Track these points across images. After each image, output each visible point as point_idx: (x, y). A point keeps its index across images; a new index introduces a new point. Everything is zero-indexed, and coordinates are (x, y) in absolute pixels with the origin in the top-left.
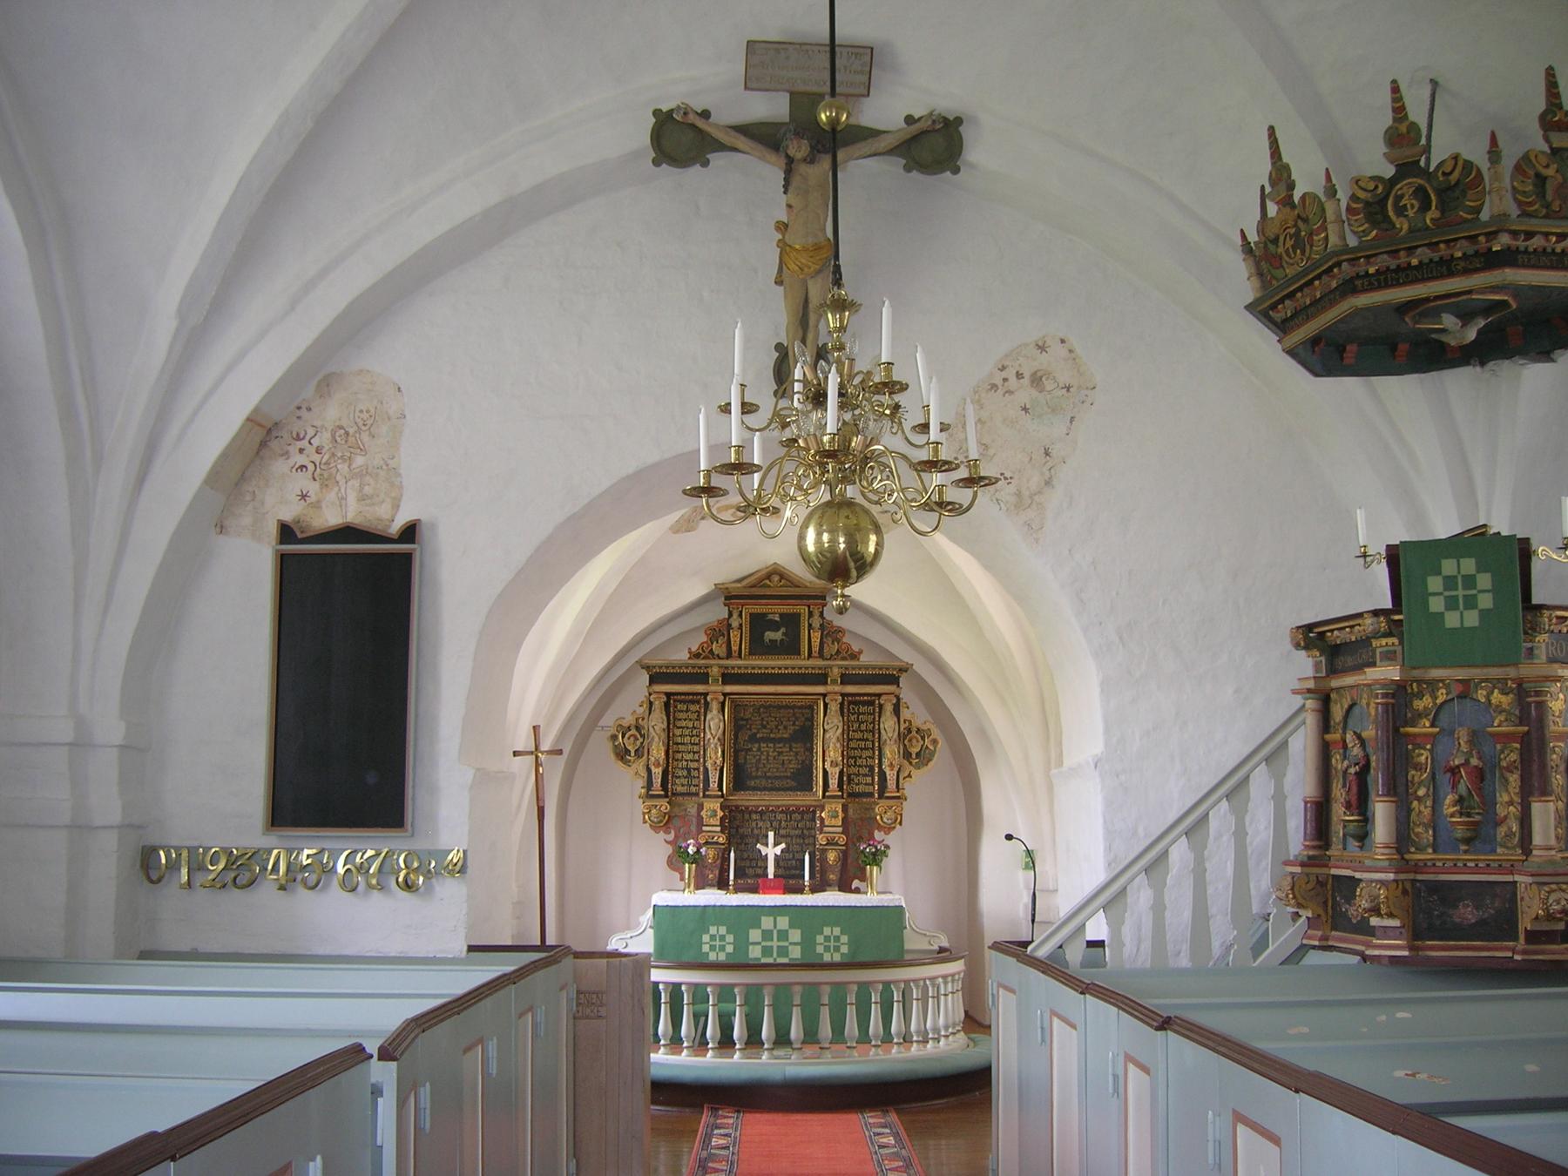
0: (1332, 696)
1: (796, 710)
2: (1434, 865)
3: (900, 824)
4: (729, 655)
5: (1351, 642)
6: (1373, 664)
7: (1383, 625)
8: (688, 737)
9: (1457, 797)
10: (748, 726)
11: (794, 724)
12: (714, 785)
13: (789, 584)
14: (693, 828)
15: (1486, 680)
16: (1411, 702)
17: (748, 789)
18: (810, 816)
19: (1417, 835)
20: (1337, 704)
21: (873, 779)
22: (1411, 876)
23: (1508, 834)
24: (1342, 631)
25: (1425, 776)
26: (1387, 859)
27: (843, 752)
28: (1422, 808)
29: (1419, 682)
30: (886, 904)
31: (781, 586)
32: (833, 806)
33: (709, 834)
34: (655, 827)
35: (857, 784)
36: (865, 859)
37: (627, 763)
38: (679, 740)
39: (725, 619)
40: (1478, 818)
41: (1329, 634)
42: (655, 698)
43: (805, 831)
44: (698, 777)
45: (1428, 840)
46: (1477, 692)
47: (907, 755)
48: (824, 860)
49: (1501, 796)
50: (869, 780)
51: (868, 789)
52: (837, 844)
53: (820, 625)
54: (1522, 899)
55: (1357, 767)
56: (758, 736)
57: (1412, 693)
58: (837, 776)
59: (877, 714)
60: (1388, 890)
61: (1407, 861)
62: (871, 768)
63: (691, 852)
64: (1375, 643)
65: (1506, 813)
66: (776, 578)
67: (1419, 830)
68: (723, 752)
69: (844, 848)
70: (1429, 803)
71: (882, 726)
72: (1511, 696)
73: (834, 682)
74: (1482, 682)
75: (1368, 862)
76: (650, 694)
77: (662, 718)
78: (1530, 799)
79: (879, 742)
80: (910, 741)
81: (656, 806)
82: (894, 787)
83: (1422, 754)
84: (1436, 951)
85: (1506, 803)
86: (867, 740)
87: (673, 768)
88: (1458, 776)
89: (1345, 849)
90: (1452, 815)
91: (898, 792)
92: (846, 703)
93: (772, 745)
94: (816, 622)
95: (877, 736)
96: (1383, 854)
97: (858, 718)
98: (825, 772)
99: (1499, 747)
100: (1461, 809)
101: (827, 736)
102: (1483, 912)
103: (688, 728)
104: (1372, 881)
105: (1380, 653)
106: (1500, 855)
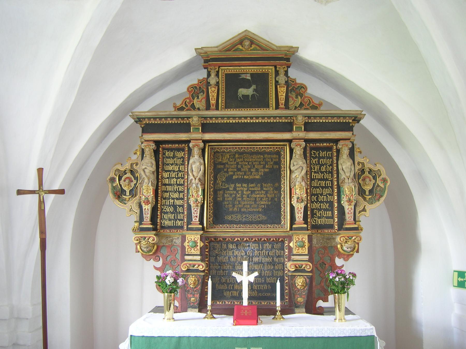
1: (266, 156)
3: (358, 251)
4: (208, 107)
8: (175, 180)
10: (225, 170)
11: (264, 167)
12: (195, 219)
13: (258, 48)
14: (178, 256)
17: (223, 223)
18: (279, 245)
21: (333, 214)
27: (307, 189)
30: (358, 335)
31: (251, 50)
32: (300, 237)
33: (191, 262)
34: (146, 256)
35: (319, 218)
36: (333, 287)
37: (123, 201)
38: (167, 181)
39: (204, 78)
42: (145, 146)
43: (275, 259)
44: (183, 213)
47: (361, 192)
48: (292, 285)
50: (329, 214)
51: (330, 221)
52: (304, 271)
53: (286, 82)
56: (234, 177)
58: (302, 211)
59: (335, 158)
62: (331, 204)
63: (168, 283)
66: (247, 43)
68: (204, 191)
69: (310, 274)
71: (340, 167)
73: (299, 129)
76: (142, 143)
77: (152, 163)
79: (338, 181)
80: (364, 180)
81: (145, 238)
82: (352, 220)
86: (327, 180)
87: (161, 205)
91: (355, 223)
92: (308, 149)
93: (246, 185)
94: (282, 79)
95: (335, 176)
97: (319, 161)
98: (292, 208)
101: (293, 176)
103: (174, 171)
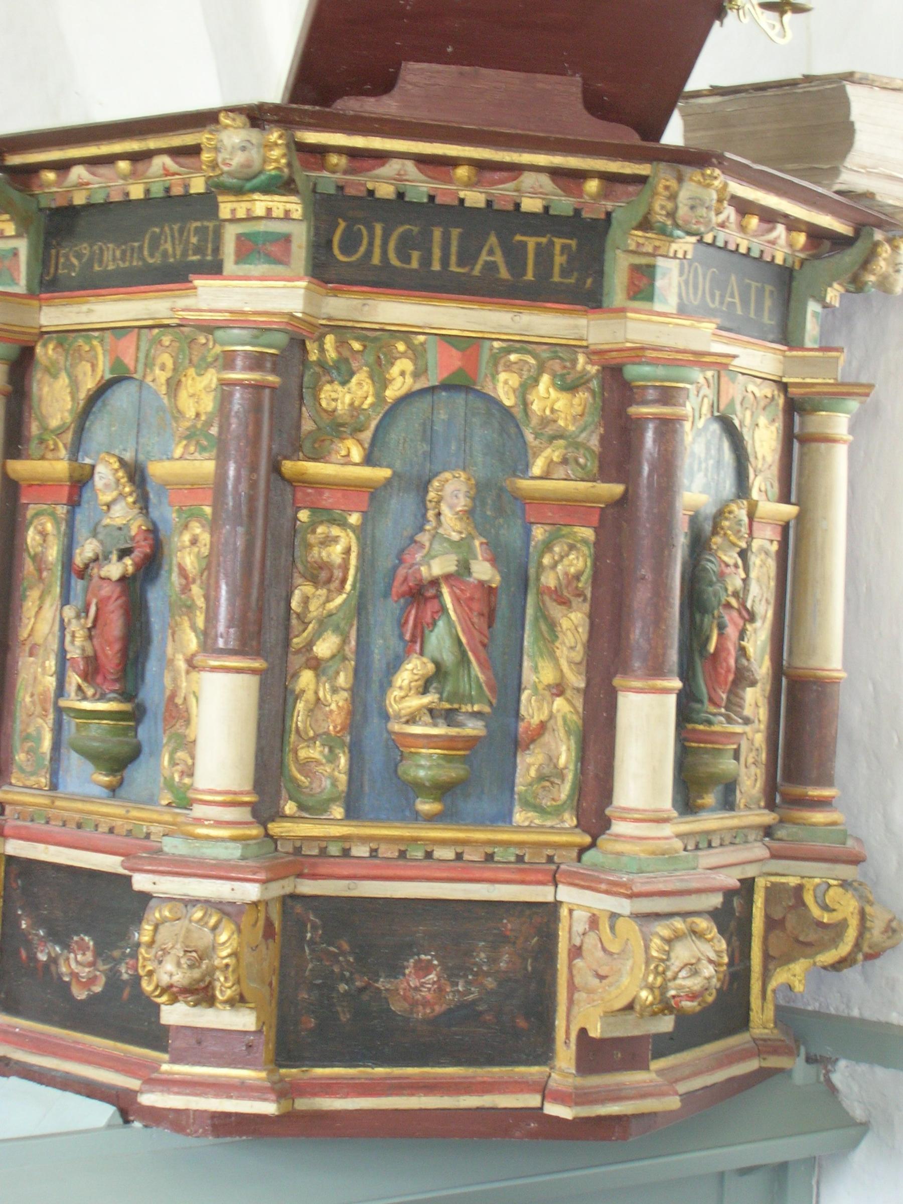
0: (39, 350)
2: (346, 853)
5: (127, 203)
6: (215, 269)
7: (276, 153)
9: (431, 667)
15: (523, 346)
16: (316, 390)
19: (305, 766)
20: (55, 376)
22: (286, 886)
23: (546, 771)
24: (103, 170)
25: (339, 600)
26: (234, 839)
28: (324, 692)
29: (341, 331)
40: (473, 728)
41: (50, 176)
45: (334, 782)
46: (494, 376)
49: (536, 669)
54: (576, 952)
55: (128, 561)
57: (321, 363)
60: (239, 931)
61: (273, 839)
64: (226, 207)
65: (544, 716)
67: (315, 752)
70: (343, 680)
72: (583, 396)
74: (509, 351)
75: (173, 846)
78: (617, 681)
83: (335, 540)
84: (346, 1096)
85: (549, 687)
88: (431, 607)
89: (54, 786)
90: (412, 719)
96: (219, 824)
99: (539, 533)
100: (441, 699)
102: (469, 983)
104: (191, 902)
105: (239, 237)
106: (520, 829)
